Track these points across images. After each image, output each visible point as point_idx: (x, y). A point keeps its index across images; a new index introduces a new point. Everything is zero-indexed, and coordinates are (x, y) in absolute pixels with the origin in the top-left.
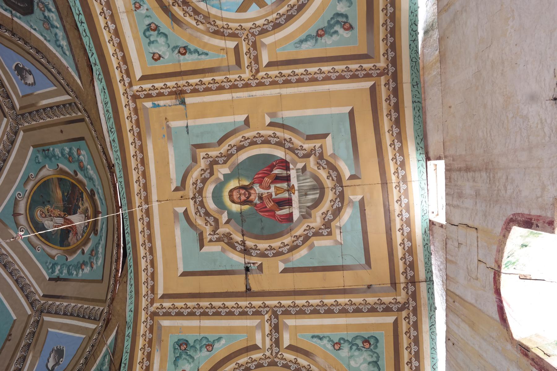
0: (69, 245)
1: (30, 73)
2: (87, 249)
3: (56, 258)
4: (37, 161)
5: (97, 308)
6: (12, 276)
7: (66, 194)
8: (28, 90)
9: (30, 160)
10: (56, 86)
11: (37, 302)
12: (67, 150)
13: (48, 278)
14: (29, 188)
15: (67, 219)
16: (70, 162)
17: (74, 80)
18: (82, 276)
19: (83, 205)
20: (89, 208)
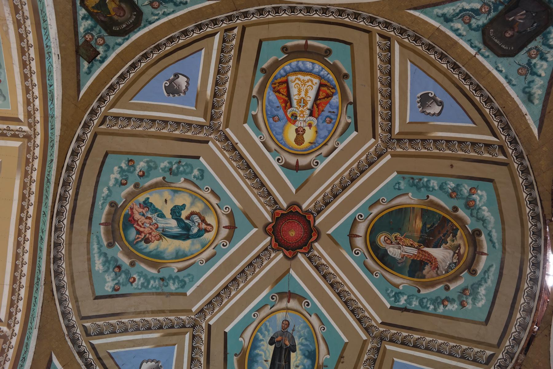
0: (424, 277)
1: (441, 104)
2: (452, 286)
3: (401, 287)
4: (397, 187)
5: (476, 350)
6: (340, 297)
7: (429, 226)
8: (422, 118)
9: (387, 183)
10: (474, 123)
11: (373, 328)
12: (451, 184)
13: (389, 306)
14: (375, 211)
15: (422, 251)
16: (451, 196)
17: (528, 127)
18: (444, 311)
19: (453, 241)
20: (462, 246)
